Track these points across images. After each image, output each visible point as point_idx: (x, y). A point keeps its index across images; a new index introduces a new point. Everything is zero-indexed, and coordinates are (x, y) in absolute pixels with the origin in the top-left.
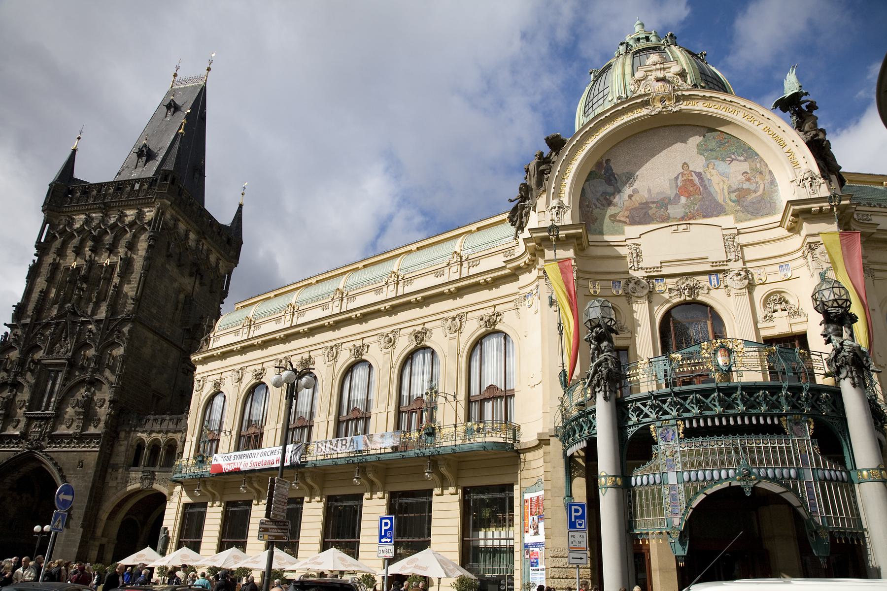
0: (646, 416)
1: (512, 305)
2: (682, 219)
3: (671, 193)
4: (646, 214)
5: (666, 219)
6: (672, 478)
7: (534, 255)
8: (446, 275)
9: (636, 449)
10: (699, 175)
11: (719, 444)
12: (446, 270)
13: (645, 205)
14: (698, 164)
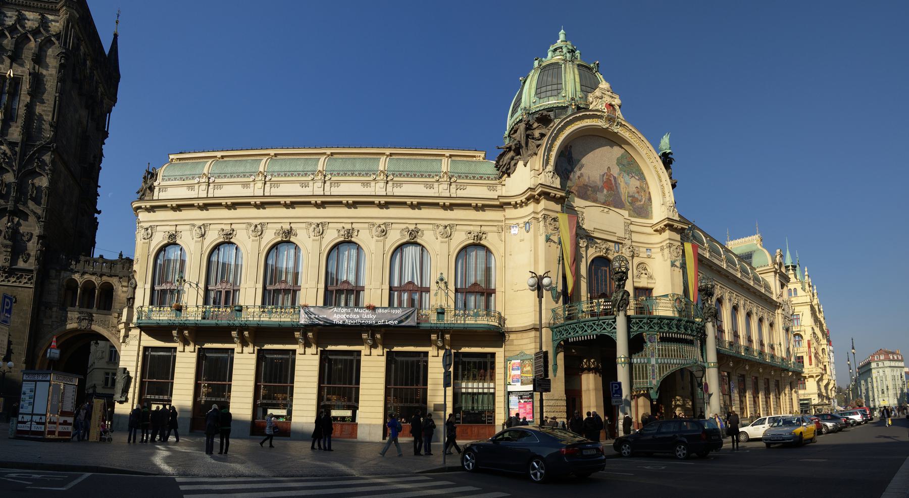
0: (641, 327)
1: (495, 229)
2: (603, 204)
3: (600, 184)
4: (586, 193)
5: (595, 200)
6: (653, 361)
7: (528, 199)
8: (436, 190)
9: (636, 345)
10: (615, 178)
11: (673, 346)
12: (436, 185)
13: (586, 186)
14: (615, 171)
